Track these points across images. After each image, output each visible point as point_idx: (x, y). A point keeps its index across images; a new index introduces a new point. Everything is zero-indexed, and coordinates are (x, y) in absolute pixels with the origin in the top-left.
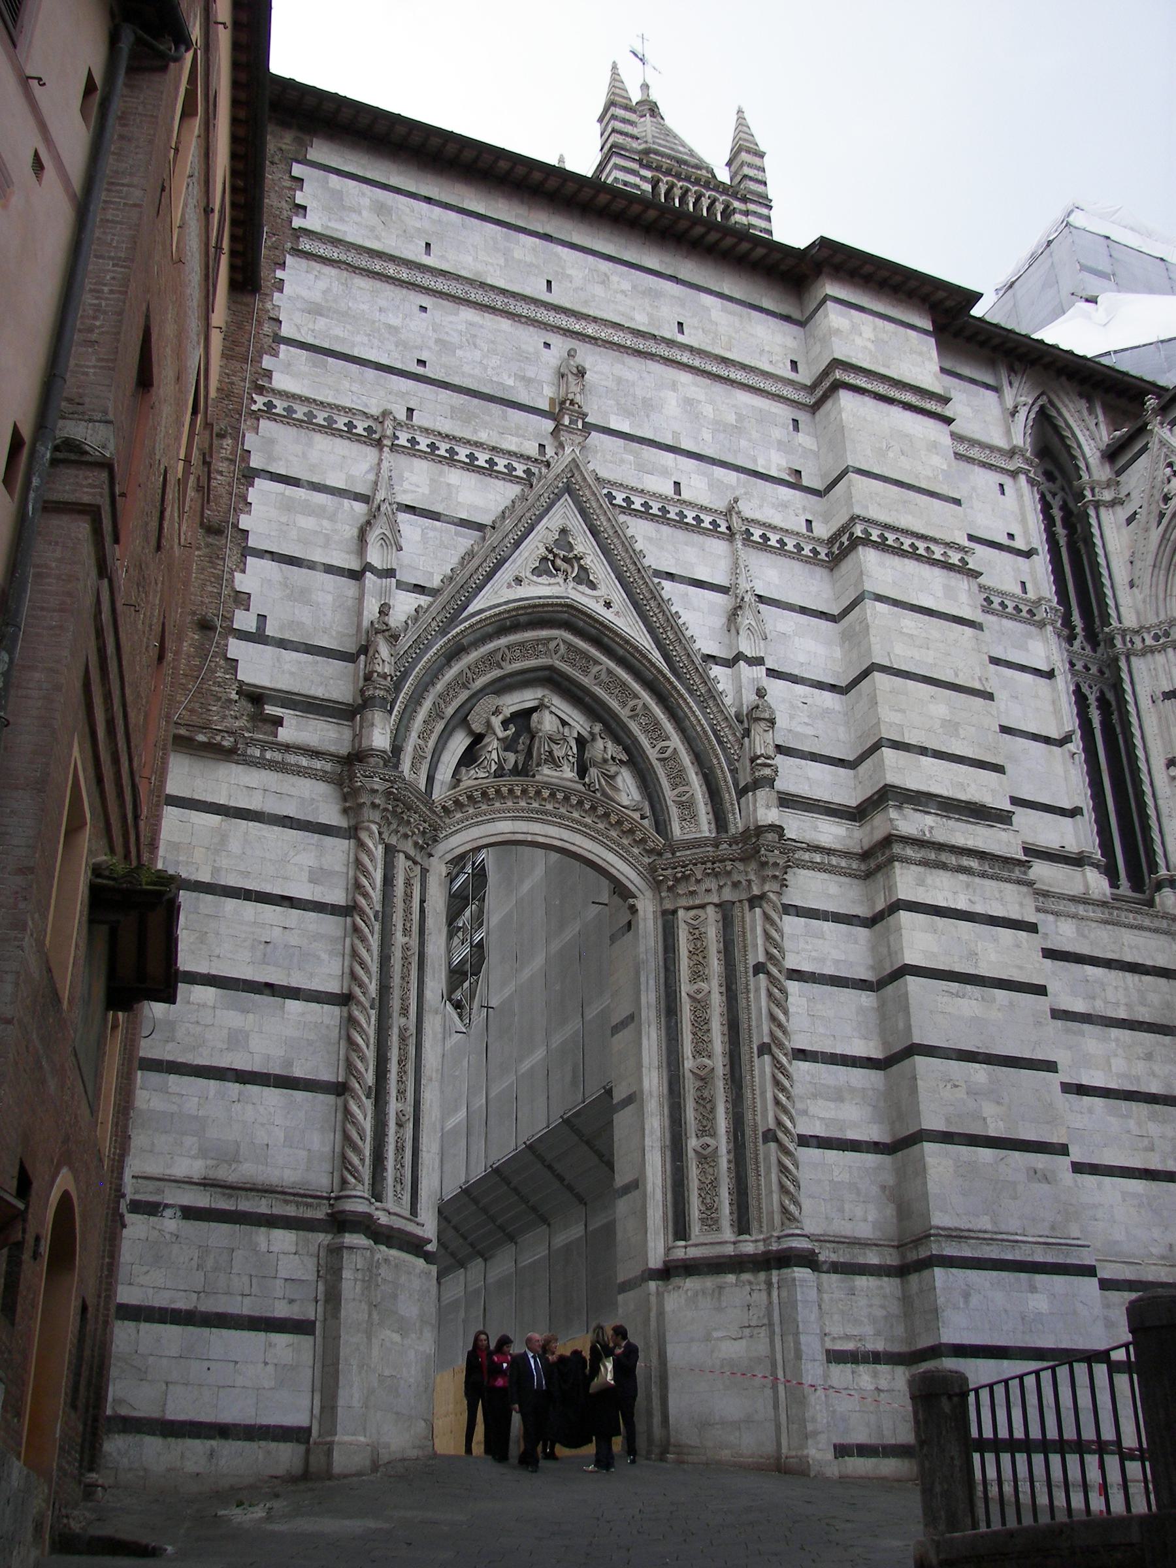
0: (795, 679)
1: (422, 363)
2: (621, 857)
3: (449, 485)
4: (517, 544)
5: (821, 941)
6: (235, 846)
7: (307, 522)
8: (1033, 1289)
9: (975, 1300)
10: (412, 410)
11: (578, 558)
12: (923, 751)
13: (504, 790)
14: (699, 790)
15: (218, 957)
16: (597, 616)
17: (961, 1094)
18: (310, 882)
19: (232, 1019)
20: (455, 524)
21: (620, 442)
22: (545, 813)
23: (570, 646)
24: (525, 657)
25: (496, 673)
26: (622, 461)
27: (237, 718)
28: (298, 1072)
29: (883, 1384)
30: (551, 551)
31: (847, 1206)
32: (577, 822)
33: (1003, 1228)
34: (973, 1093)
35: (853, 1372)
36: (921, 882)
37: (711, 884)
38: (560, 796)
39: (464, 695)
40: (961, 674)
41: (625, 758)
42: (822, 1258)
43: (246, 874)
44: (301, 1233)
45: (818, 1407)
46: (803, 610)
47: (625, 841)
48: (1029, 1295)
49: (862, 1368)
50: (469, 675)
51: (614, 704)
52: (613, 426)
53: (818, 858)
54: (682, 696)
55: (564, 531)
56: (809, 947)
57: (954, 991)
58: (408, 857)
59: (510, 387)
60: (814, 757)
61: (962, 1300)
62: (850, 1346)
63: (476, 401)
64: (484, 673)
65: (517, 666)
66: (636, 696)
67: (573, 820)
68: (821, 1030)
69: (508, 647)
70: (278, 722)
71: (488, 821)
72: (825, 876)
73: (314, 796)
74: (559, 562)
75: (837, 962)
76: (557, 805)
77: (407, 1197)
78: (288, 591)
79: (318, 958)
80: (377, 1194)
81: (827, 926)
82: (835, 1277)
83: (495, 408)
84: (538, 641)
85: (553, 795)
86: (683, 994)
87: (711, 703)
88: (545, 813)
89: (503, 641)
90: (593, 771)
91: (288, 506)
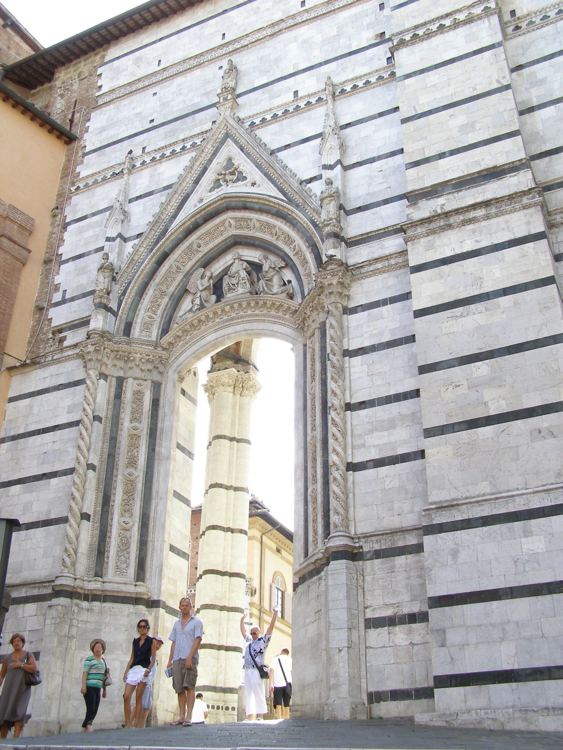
0: (372, 160)
1: (152, 121)
2: (281, 324)
3: (159, 174)
4: (197, 182)
5: (381, 320)
6: (35, 410)
7: (89, 234)
8: (527, 533)
9: (463, 556)
10: (145, 147)
11: (236, 169)
12: (442, 156)
13: (203, 318)
14: (311, 262)
15: (23, 468)
16: (239, 195)
17: (463, 390)
18: (68, 413)
19: (27, 498)
20: (161, 191)
21: (260, 91)
22: (232, 319)
23: (236, 219)
24: (212, 239)
25: (200, 255)
26: (262, 100)
27: (51, 347)
28: (53, 516)
29: (417, 639)
30: (222, 174)
31: (396, 505)
32: (252, 316)
33: (503, 487)
34: (474, 386)
35: (389, 633)
36: (430, 247)
37: (314, 315)
38: (236, 306)
39: (180, 277)
40: (478, 88)
41: (283, 264)
42: (366, 549)
43: (38, 422)
44: (39, 603)
45: (341, 665)
46: (381, 115)
47: (280, 314)
48: (523, 539)
49: (397, 629)
50: (180, 265)
51: (268, 237)
52: (256, 86)
53: (379, 265)
54: (293, 212)
55: (230, 159)
56: (371, 328)
57: (459, 314)
58: (135, 379)
59: (198, 103)
60: (386, 202)
61: (450, 558)
62: (388, 612)
63: (179, 122)
64: (190, 259)
65: (211, 246)
66: (275, 226)
67: (248, 316)
68: (379, 383)
69: (199, 238)
70: (64, 338)
71: (201, 339)
72: (385, 275)
73: (73, 369)
74: (228, 177)
75: (392, 331)
76: (237, 312)
77: (132, 571)
78: (77, 272)
79: (68, 452)
80: (99, 573)
81: (384, 309)
82: (377, 562)
83: (188, 119)
84: (217, 226)
85: (232, 307)
86: (308, 394)
87: (306, 206)
88: (232, 319)
89: (193, 238)
90: (262, 282)
91: (80, 231)
